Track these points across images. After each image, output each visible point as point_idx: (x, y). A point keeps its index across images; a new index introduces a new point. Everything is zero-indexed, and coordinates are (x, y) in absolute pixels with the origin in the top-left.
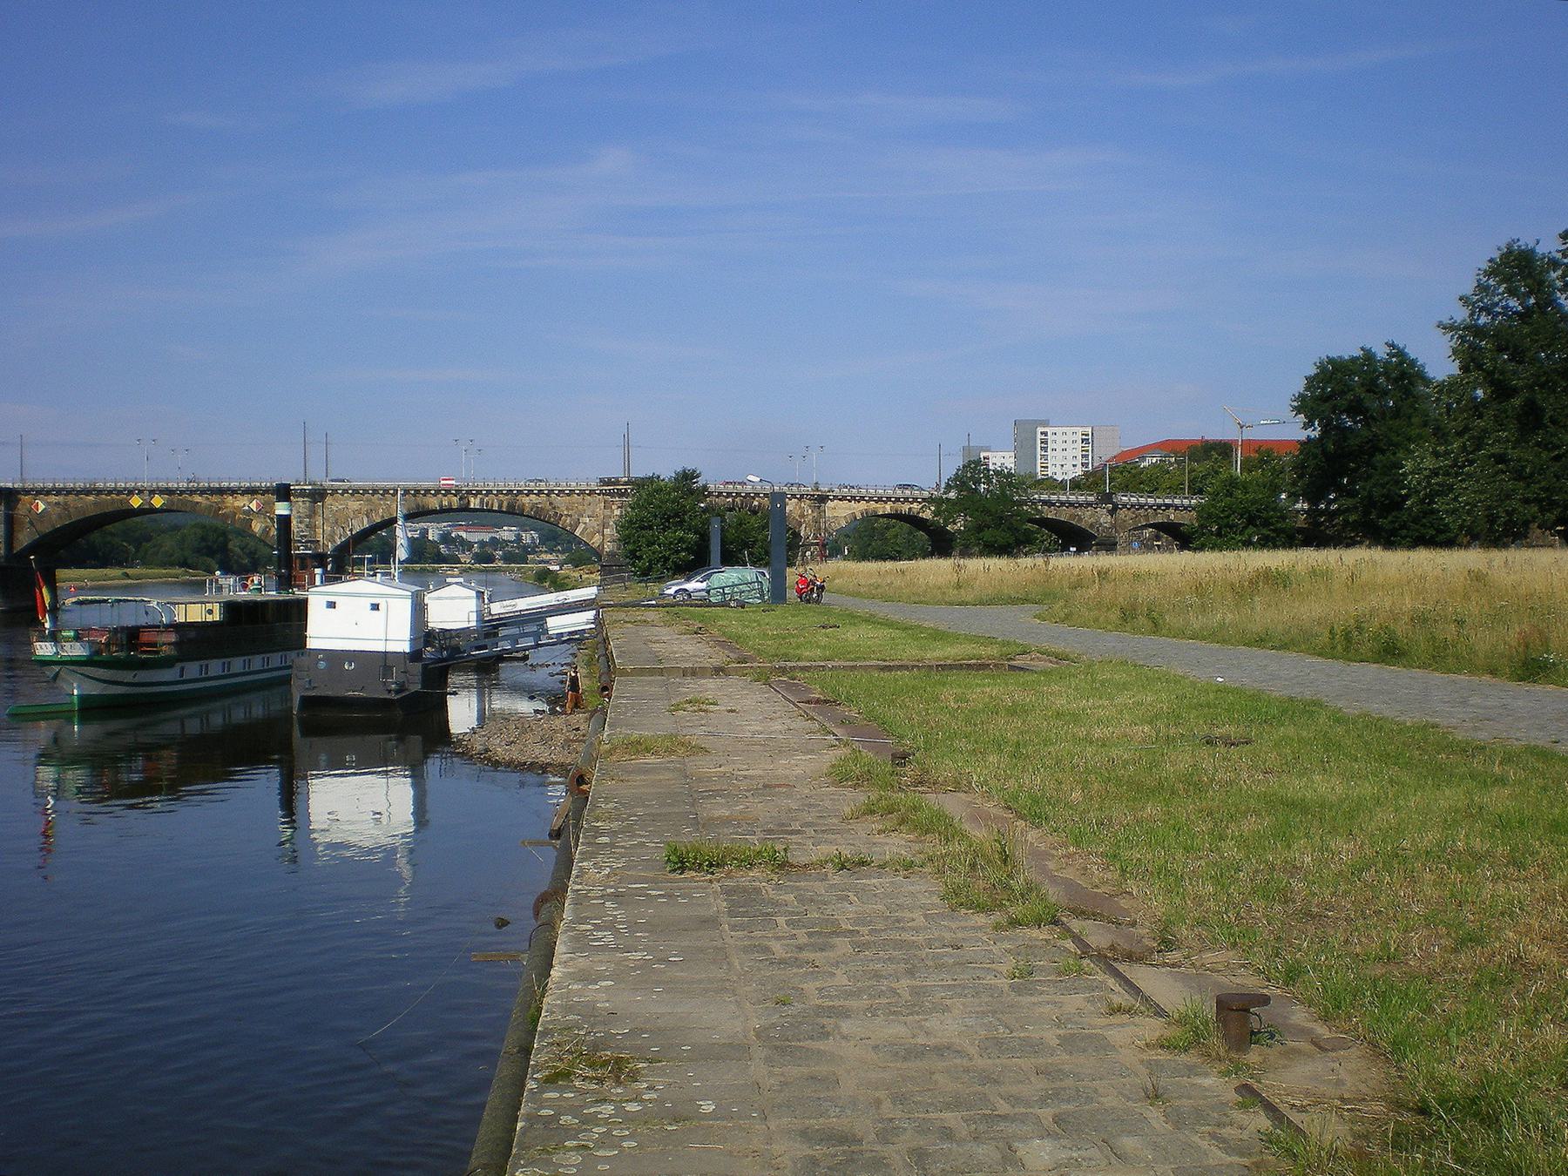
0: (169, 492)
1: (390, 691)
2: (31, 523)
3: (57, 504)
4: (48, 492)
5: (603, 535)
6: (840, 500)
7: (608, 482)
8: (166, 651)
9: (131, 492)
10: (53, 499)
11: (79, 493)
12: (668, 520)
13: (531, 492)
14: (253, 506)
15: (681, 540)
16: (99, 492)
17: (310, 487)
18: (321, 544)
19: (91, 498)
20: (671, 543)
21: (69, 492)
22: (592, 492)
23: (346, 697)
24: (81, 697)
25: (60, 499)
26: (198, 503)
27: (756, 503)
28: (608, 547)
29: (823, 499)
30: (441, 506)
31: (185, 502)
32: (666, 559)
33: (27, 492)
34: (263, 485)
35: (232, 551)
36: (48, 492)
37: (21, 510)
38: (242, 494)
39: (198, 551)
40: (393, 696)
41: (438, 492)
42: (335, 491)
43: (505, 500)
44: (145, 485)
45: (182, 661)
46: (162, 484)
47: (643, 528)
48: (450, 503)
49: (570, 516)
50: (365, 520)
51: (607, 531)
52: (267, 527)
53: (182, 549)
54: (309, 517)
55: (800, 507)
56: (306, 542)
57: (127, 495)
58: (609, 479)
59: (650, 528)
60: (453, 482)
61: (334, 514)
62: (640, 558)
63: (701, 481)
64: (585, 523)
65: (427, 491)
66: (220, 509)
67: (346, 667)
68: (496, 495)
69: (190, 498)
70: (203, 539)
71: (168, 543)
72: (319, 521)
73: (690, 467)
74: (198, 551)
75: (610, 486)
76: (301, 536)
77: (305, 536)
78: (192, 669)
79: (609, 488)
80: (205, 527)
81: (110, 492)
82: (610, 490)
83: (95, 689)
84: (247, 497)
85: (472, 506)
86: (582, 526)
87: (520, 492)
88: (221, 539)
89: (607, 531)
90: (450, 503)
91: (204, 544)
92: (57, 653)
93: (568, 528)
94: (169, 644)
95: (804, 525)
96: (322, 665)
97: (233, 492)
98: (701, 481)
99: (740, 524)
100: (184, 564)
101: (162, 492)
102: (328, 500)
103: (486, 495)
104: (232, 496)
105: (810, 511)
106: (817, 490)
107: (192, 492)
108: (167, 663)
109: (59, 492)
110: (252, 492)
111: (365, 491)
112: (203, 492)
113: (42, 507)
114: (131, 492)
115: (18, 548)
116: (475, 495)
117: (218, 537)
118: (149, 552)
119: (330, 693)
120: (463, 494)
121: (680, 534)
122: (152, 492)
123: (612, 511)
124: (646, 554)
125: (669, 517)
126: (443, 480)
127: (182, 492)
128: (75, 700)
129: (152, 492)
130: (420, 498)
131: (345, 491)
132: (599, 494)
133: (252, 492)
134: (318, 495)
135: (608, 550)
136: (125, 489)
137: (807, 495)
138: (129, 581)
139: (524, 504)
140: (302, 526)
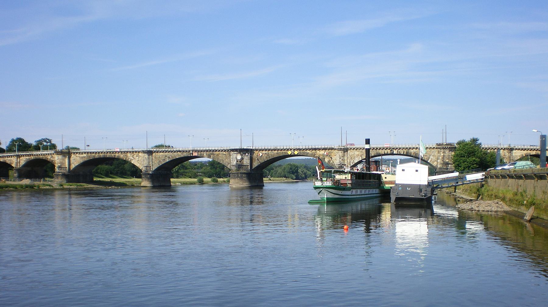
0: (300, 149)
1: (422, 196)
3: (266, 153)
4: (263, 150)
5: (437, 162)
6: (518, 150)
7: (440, 145)
9: (288, 150)
10: (264, 152)
11: (272, 150)
12: (470, 154)
13: (413, 148)
15: (474, 161)
16: (278, 150)
17: (343, 147)
18: (346, 165)
19: (276, 151)
20: (471, 161)
21: (269, 150)
22: (434, 148)
23: (410, 198)
25: (267, 152)
27: (489, 151)
28: (439, 166)
29: (512, 149)
31: (304, 153)
32: (469, 167)
33: (257, 150)
35: (299, 172)
36: (263, 150)
37: (255, 155)
38: (322, 150)
39: (289, 172)
40: (423, 197)
41: (383, 148)
42: (351, 149)
43: (405, 151)
44: (292, 148)
45: (352, 189)
46: (298, 147)
47: (461, 157)
48: (387, 152)
49: (427, 156)
50: (360, 158)
51: (439, 161)
53: (284, 172)
55: (504, 153)
56: (342, 165)
57: (287, 151)
58: (440, 144)
59: (464, 157)
60: (388, 145)
62: (461, 167)
63: (479, 142)
64: (431, 158)
65: (380, 148)
66: (315, 154)
67: (408, 189)
68: (402, 149)
69: (306, 151)
70: (291, 169)
71: (280, 170)
72: (346, 158)
73: (475, 137)
74: (289, 172)
75: (440, 147)
76: (340, 163)
78: (354, 192)
79: (440, 146)
80: (291, 165)
81: (282, 150)
82: (439, 147)
85: (394, 153)
86: (430, 159)
87: (410, 148)
88: (296, 169)
89: (439, 161)
90: (387, 152)
91: (291, 170)
93: (426, 160)
94: (349, 184)
95: (505, 159)
96: (400, 188)
97: (319, 149)
98: (479, 142)
99: (492, 156)
100: (285, 177)
101: (297, 150)
102: (349, 151)
103: (399, 149)
104: (319, 150)
105: (507, 154)
106: (510, 147)
107: (307, 149)
109: (266, 150)
110: (325, 149)
112: (310, 149)
113: (261, 155)
114: (288, 150)
115: (254, 167)
116: (396, 149)
117: (295, 168)
119: (405, 197)
120: (392, 149)
121: (474, 158)
122: (294, 150)
123: (441, 154)
124: (463, 165)
125: (471, 153)
127: (304, 150)
130: (378, 150)
131: (354, 149)
132: (436, 149)
134: (345, 150)
135: (439, 167)
136: (286, 149)
137: (507, 148)
138: (271, 181)
139: (411, 152)
140: (340, 160)
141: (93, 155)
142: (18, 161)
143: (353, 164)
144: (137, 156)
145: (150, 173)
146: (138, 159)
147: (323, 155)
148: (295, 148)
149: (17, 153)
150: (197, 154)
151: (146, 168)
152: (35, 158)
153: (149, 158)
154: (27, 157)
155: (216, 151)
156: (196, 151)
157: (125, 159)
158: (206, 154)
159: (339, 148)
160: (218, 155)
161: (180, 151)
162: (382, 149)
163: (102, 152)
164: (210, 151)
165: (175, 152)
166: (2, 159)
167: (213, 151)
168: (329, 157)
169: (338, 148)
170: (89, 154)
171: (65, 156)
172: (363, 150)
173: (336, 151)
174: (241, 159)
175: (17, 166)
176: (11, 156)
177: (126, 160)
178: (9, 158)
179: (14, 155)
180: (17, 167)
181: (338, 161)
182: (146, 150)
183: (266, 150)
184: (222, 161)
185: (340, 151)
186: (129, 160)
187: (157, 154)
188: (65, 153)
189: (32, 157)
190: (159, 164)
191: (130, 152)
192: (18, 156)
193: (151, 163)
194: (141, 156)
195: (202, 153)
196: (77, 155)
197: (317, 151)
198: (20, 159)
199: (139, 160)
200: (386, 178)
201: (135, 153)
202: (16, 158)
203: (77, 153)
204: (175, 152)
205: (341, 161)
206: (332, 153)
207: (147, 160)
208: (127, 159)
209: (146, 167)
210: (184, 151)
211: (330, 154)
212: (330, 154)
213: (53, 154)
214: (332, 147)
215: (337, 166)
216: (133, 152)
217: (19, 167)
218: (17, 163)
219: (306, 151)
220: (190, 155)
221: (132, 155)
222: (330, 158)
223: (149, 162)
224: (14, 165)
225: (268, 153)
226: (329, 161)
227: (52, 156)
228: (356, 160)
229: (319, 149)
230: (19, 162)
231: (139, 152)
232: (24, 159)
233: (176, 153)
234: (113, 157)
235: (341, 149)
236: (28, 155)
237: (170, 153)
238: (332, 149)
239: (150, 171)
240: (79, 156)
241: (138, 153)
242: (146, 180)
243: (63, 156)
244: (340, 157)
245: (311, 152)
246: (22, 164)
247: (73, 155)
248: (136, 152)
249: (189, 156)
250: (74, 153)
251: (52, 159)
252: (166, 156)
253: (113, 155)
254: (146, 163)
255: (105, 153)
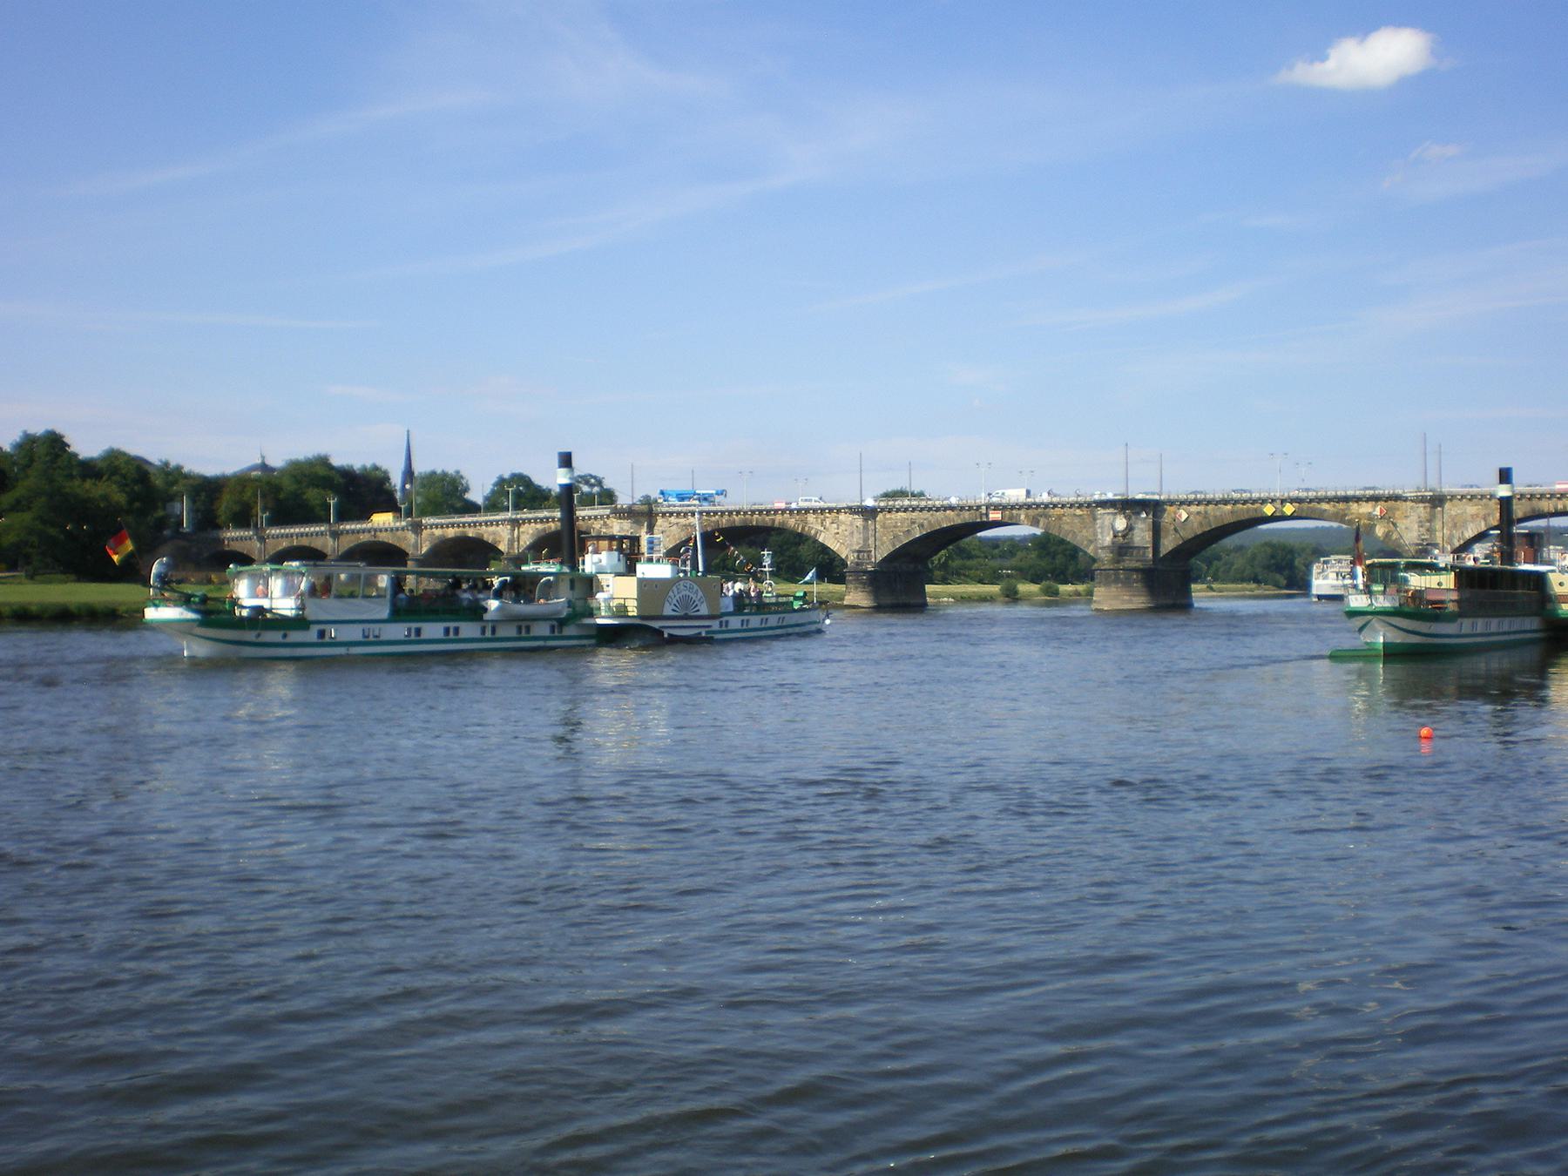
2: (1176, 530)
3: (1199, 513)
4: (1190, 503)
8: (1452, 607)
9: (1264, 501)
10: (1194, 509)
11: (1217, 503)
14: (1377, 512)
16: (1236, 502)
17: (1431, 494)
18: (1441, 546)
19: (1229, 507)
21: (1209, 502)
24: (1385, 644)
25: (1201, 508)
26: (1326, 510)
30: (1556, 509)
31: (1313, 510)
33: (1172, 503)
34: (1386, 492)
36: (1190, 503)
37: (1166, 519)
41: (1552, 495)
42: (1453, 497)
46: (1294, 494)
50: (1483, 523)
52: (1389, 532)
54: (1429, 521)
56: (1427, 544)
61: (1453, 520)
65: (1542, 496)
69: (1319, 506)
70: (1273, 557)
71: (1239, 562)
72: (1438, 525)
74: (1268, 568)
76: (1423, 540)
77: (1426, 539)
78: (1466, 625)
81: (1245, 502)
83: (1397, 638)
84: (1371, 504)
88: (1289, 556)
91: (1273, 561)
92: (1371, 604)
97: (1358, 499)
100: (1256, 581)
101: (1292, 501)
102: (1447, 505)
104: (1357, 502)
107: (1320, 500)
108: (1452, 618)
109: (1199, 503)
110: (1375, 499)
111: (1483, 496)
112: (1329, 500)
113: (1184, 516)
115: (1163, 551)
118: (1222, 570)
122: (1283, 502)
126: (1559, 484)
127: (1311, 501)
128: (1381, 647)
129: (1283, 502)
130: (1535, 502)
131: (1463, 497)
133: (1375, 499)
134: (1437, 501)
136: (1260, 499)
141: (713, 519)
142: (515, 536)
143: (1462, 542)
144: (833, 523)
145: (870, 568)
146: (836, 531)
147: (1370, 517)
148: (1286, 495)
149: (509, 515)
150: (1000, 515)
151: (858, 556)
152: (458, 535)
153: (866, 528)
154: (539, 526)
155: (1055, 506)
156: (997, 507)
157: (800, 529)
158: (1027, 516)
159: (1419, 494)
160: (1059, 517)
161: (952, 508)
162: (1548, 496)
163: (738, 513)
164: (1038, 506)
165: (938, 510)
166: (472, 529)
167: (1046, 506)
168: (1388, 523)
169: (1415, 494)
170: (705, 517)
171: (639, 523)
172: (1490, 499)
173: (1408, 503)
174: (1125, 529)
175: (513, 549)
176: (497, 521)
177: (805, 533)
178: (491, 529)
179: (505, 520)
180: (511, 551)
181: (1415, 534)
182: (859, 504)
183: (1199, 503)
184: (1070, 535)
185: (1421, 505)
186: (813, 532)
187: (888, 516)
188: (638, 513)
189: (552, 525)
190: (894, 545)
191: (815, 511)
192: (515, 523)
193: (871, 541)
194: (843, 523)
195: (1014, 512)
196: (673, 519)
197: (1351, 503)
198: (521, 530)
199: (838, 533)
200: (1561, 584)
201: (828, 515)
202: (509, 527)
203: (671, 514)
204: (938, 510)
205: (1423, 534)
206: (1398, 509)
207: (860, 533)
208: (807, 529)
209: (859, 552)
210: (962, 508)
211: (1390, 514)
212: (1390, 514)
213: (608, 517)
214: (1396, 492)
215: (1413, 549)
216: (823, 510)
217: (516, 551)
218: (511, 542)
219: (1319, 506)
220: (981, 518)
221: (819, 520)
222: (1391, 525)
223: (866, 540)
224: (503, 547)
225: (1206, 512)
226: (1387, 535)
227: (605, 522)
228: (1470, 531)
229: (1358, 499)
230: (516, 539)
231: (839, 511)
232: (531, 532)
233: (940, 515)
234: (769, 524)
235: (1422, 500)
236: (541, 520)
237: (926, 514)
238: (1397, 498)
239: (868, 564)
240: (677, 524)
241: (837, 513)
242: (856, 588)
243: (634, 522)
244: (1421, 522)
245: (1334, 506)
246: (525, 542)
247: (660, 521)
248: (831, 510)
249: (979, 520)
250: (664, 514)
251: (604, 530)
252: (914, 523)
253: (767, 518)
254: (857, 542)
255: (745, 513)
